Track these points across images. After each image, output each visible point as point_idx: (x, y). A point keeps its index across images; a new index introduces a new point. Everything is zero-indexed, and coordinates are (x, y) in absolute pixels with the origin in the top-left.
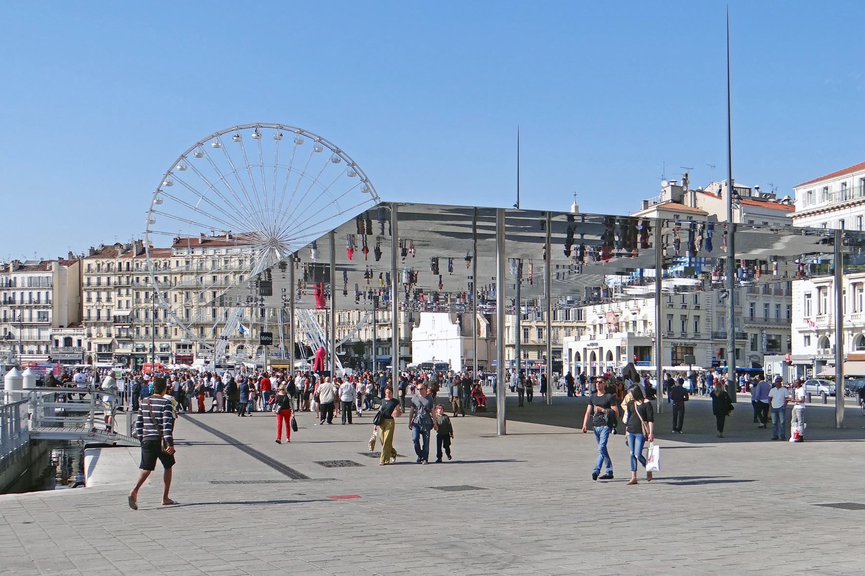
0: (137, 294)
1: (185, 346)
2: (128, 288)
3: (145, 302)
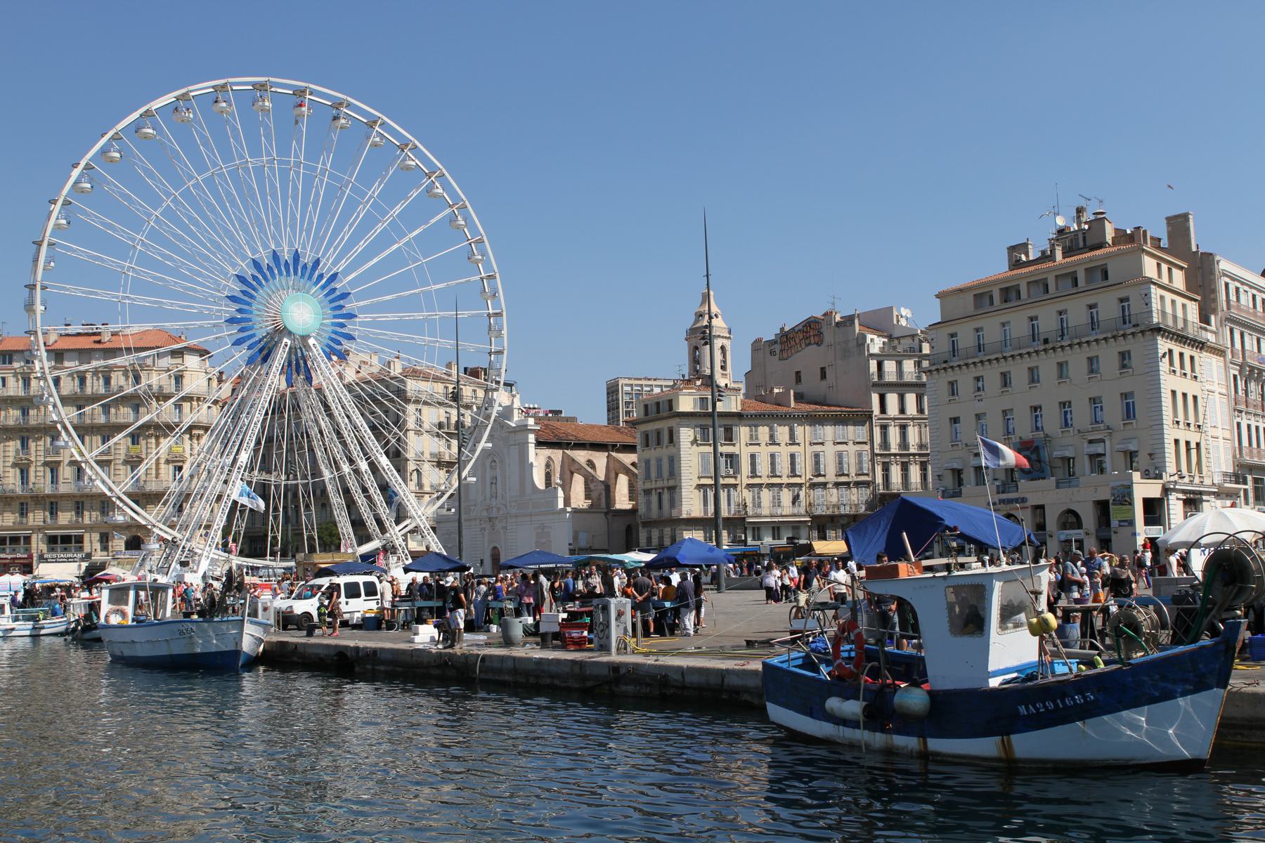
1: (15, 540)
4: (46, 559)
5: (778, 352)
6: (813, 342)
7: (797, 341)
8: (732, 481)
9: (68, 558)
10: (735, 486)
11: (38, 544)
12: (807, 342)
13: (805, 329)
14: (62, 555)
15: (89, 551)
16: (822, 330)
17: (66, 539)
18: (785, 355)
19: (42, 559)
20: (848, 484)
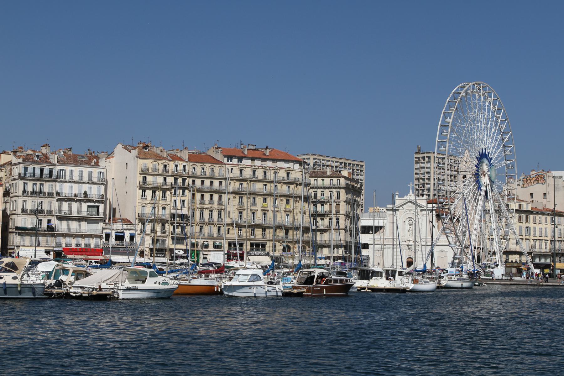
0: (193, 195)
2: (184, 189)
3: (201, 203)
4: (250, 254)
5: (521, 184)
6: (540, 182)
7: (532, 181)
8: (528, 237)
9: (259, 254)
10: (529, 239)
11: (247, 247)
12: (537, 182)
13: (536, 177)
14: (257, 253)
15: (268, 251)
16: (545, 178)
17: (258, 245)
18: (525, 186)
19: (249, 254)
20: (561, 241)
